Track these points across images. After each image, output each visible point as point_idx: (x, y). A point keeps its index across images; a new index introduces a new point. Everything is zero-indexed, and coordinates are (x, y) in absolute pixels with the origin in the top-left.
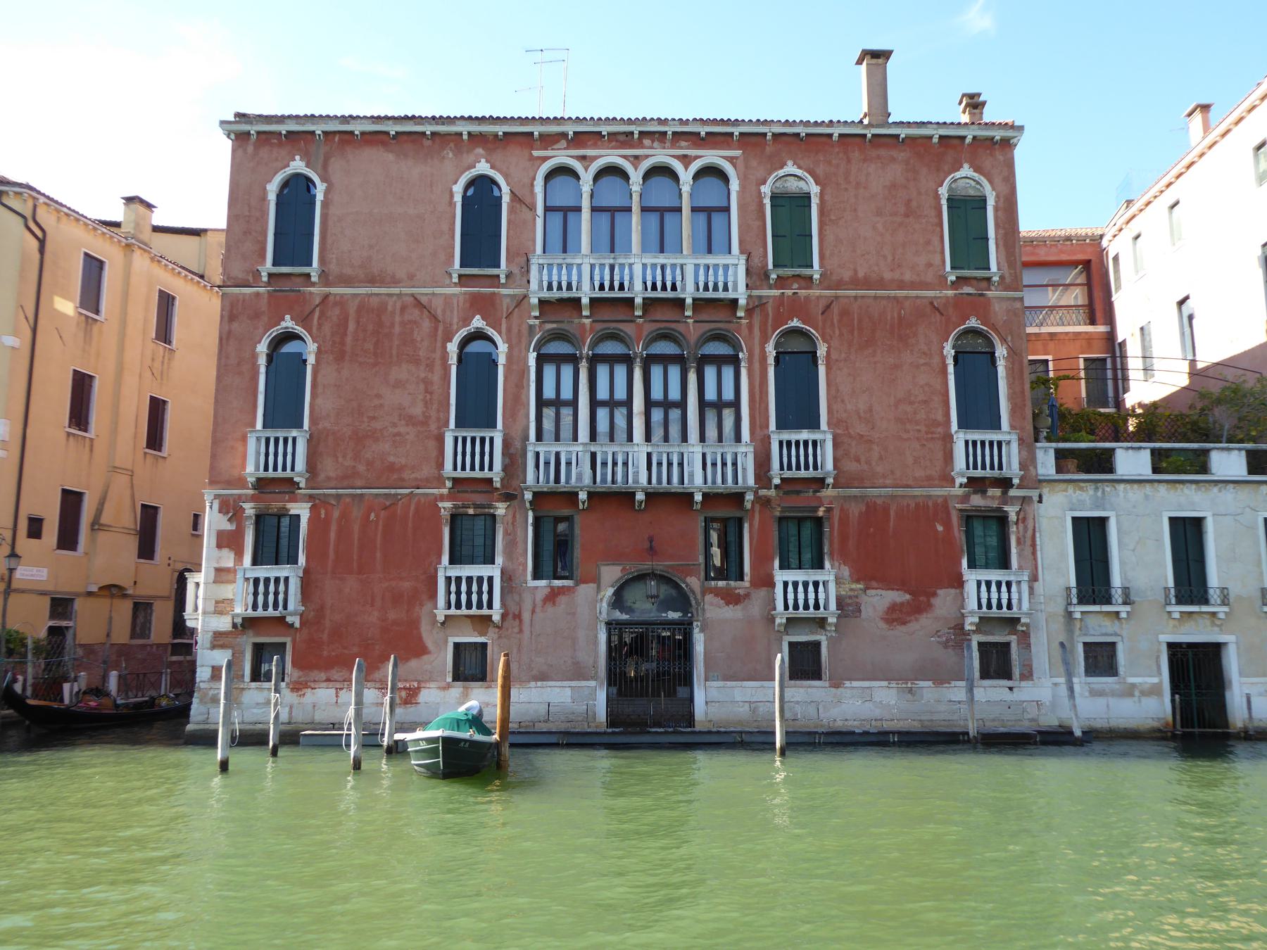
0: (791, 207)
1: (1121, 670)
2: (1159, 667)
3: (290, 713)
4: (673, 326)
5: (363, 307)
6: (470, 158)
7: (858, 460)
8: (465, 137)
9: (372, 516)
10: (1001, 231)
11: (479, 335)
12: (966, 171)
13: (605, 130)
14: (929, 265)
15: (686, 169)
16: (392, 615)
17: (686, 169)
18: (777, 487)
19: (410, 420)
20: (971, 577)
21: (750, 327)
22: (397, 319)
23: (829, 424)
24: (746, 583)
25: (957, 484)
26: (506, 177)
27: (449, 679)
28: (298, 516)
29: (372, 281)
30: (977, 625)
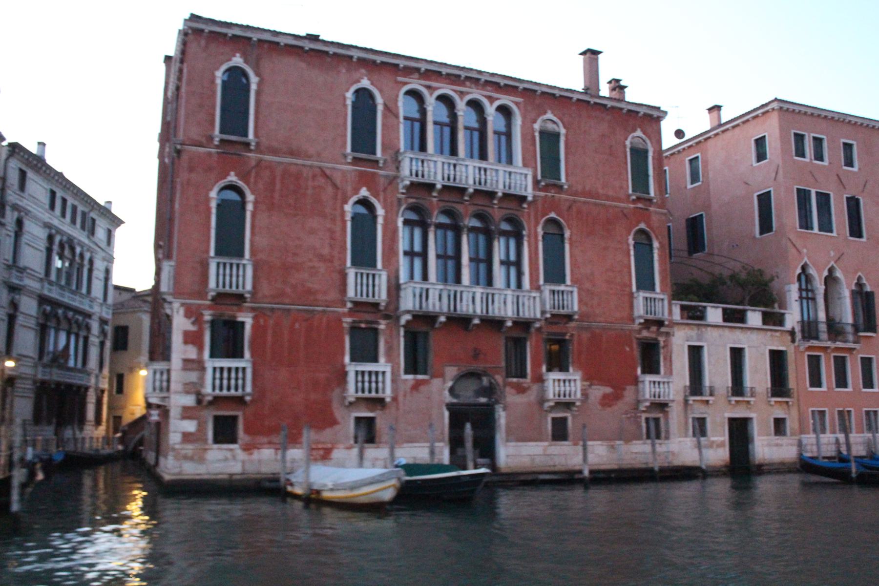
0: (550, 139)
3: (243, 466)
5: (286, 173)
6: (356, 75)
8: (354, 60)
9: (297, 326)
12: (639, 133)
13: (444, 71)
14: (621, 188)
16: (313, 396)
19: (321, 258)
22: (310, 183)
23: (572, 281)
27: (352, 442)
28: (243, 323)
29: (292, 153)
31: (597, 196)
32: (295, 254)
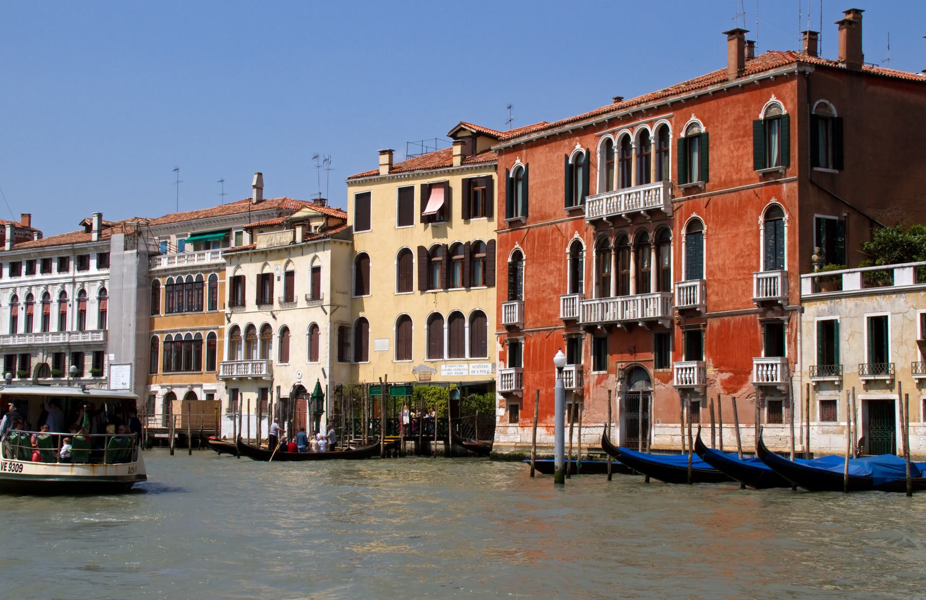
7: (717, 294)
31: (732, 183)
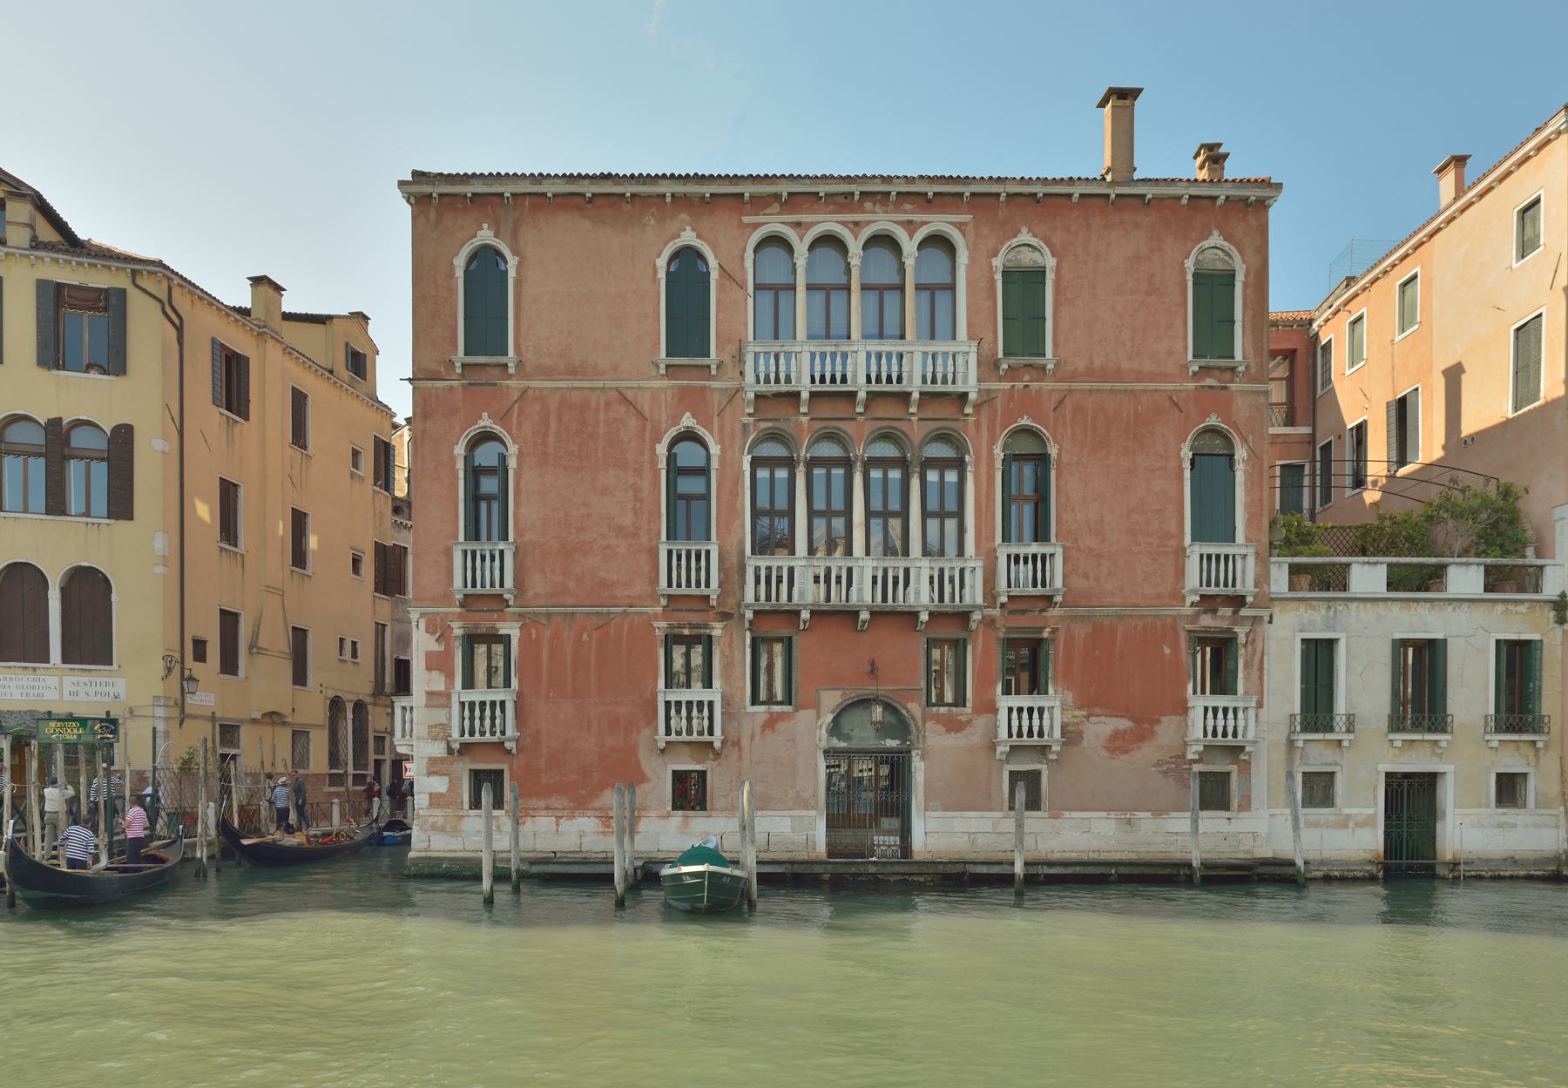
1: (1338, 800)
2: (1375, 797)
4: (896, 424)
6: (672, 226)
7: (1086, 576)
8: (668, 200)
10: (1250, 312)
11: (689, 436)
12: (1216, 239)
13: (822, 189)
14: (1170, 353)
15: (911, 237)
17: (911, 237)
18: (1003, 605)
19: (620, 531)
20: (1199, 703)
21: (978, 424)
22: (602, 416)
24: (968, 709)
25: (1188, 603)
26: (714, 248)
27: (669, 808)
30: (1200, 754)
32: (581, 529)
